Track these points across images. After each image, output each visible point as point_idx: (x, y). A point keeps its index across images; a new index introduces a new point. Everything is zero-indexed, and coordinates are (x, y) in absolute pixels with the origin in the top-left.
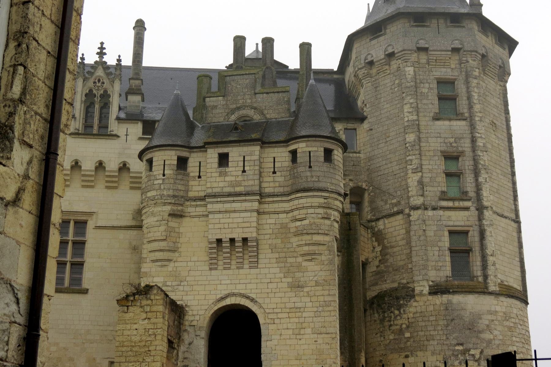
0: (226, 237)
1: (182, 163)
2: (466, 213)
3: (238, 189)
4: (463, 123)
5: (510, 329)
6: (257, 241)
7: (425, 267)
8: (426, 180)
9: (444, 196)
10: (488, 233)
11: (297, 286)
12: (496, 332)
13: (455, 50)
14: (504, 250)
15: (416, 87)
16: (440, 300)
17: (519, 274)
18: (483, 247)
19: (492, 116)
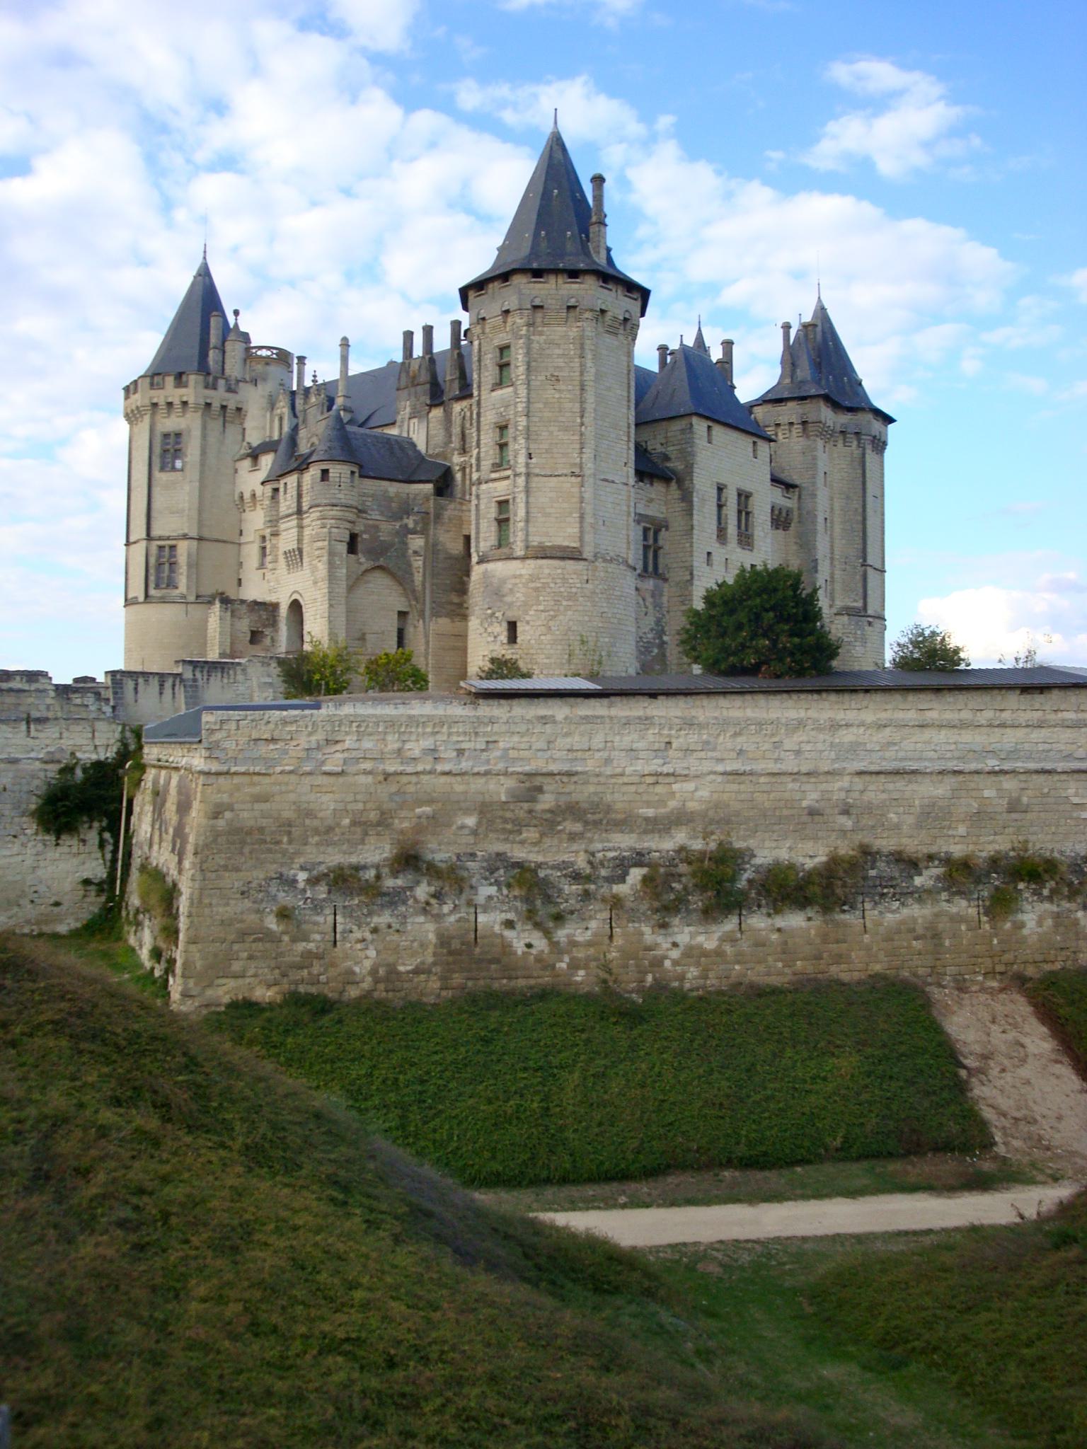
0: (287, 549)
1: (276, 490)
2: (506, 483)
3: (290, 511)
4: (511, 389)
5: (536, 589)
6: (300, 551)
7: (477, 538)
8: (482, 455)
9: (497, 467)
10: (518, 500)
11: (315, 583)
12: (518, 595)
13: (507, 312)
14: (548, 510)
15: (479, 361)
16: (484, 566)
17: (577, 530)
18: (515, 515)
19: (551, 370)
